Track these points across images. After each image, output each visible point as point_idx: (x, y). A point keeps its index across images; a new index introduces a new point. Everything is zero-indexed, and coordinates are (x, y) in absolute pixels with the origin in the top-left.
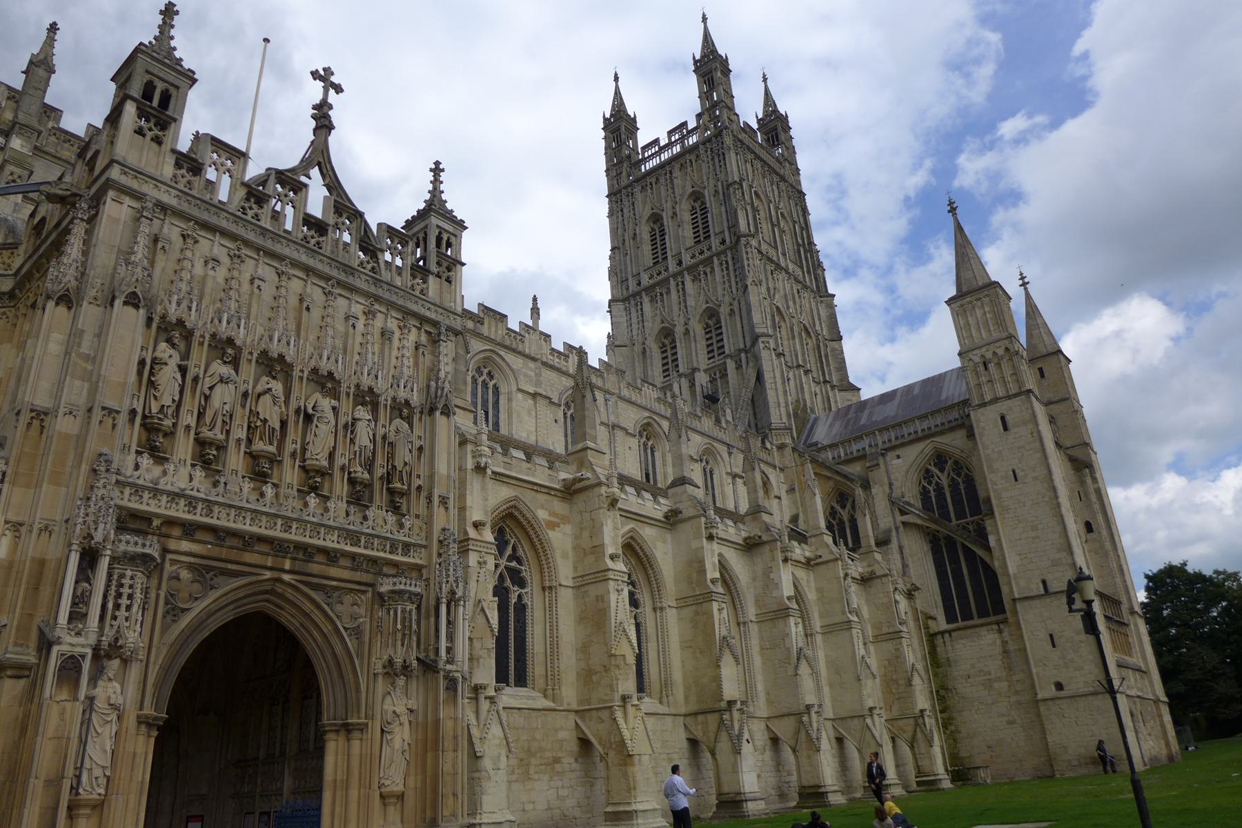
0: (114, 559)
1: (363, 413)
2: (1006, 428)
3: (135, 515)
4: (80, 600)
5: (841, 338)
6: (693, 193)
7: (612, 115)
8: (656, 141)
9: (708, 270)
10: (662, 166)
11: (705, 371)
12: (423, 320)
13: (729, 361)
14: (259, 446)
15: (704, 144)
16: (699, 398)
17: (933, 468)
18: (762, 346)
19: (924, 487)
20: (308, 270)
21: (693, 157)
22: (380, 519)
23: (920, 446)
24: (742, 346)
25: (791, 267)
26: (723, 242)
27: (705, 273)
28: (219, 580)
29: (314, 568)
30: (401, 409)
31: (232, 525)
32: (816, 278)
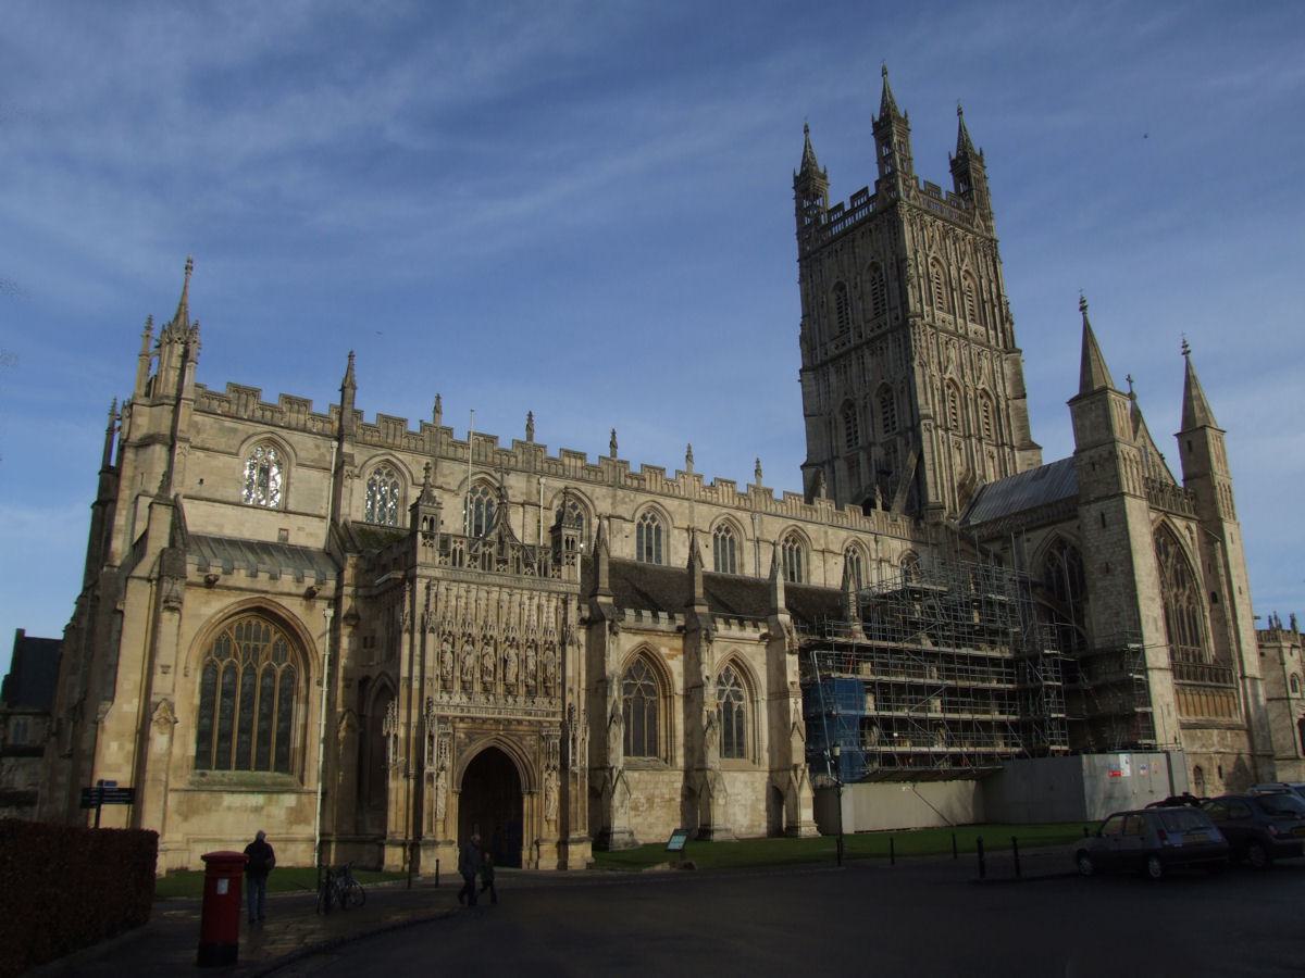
0: (439, 736)
1: (531, 653)
2: (1104, 526)
3: (442, 717)
4: (431, 753)
5: (1024, 396)
6: (873, 263)
7: (802, 174)
8: (840, 207)
9: (884, 346)
10: (845, 233)
11: (882, 445)
12: (559, 593)
13: (899, 439)
14: (487, 679)
15: (881, 213)
16: (874, 472)
17: (1056, 552)
18: (923, 427)
19: (1048, 569)
20: (501, 586)
21: (872, 226)
22: (541, 702)
23: (1042, 533)
24: (909, 424)
25: (972, 327)
26: (897, 318)
27: (881, 348)
28: (476, 736)
29: (513, 727)
30: (550, 647)
31: (478, 715)
32: (1003, 332)
